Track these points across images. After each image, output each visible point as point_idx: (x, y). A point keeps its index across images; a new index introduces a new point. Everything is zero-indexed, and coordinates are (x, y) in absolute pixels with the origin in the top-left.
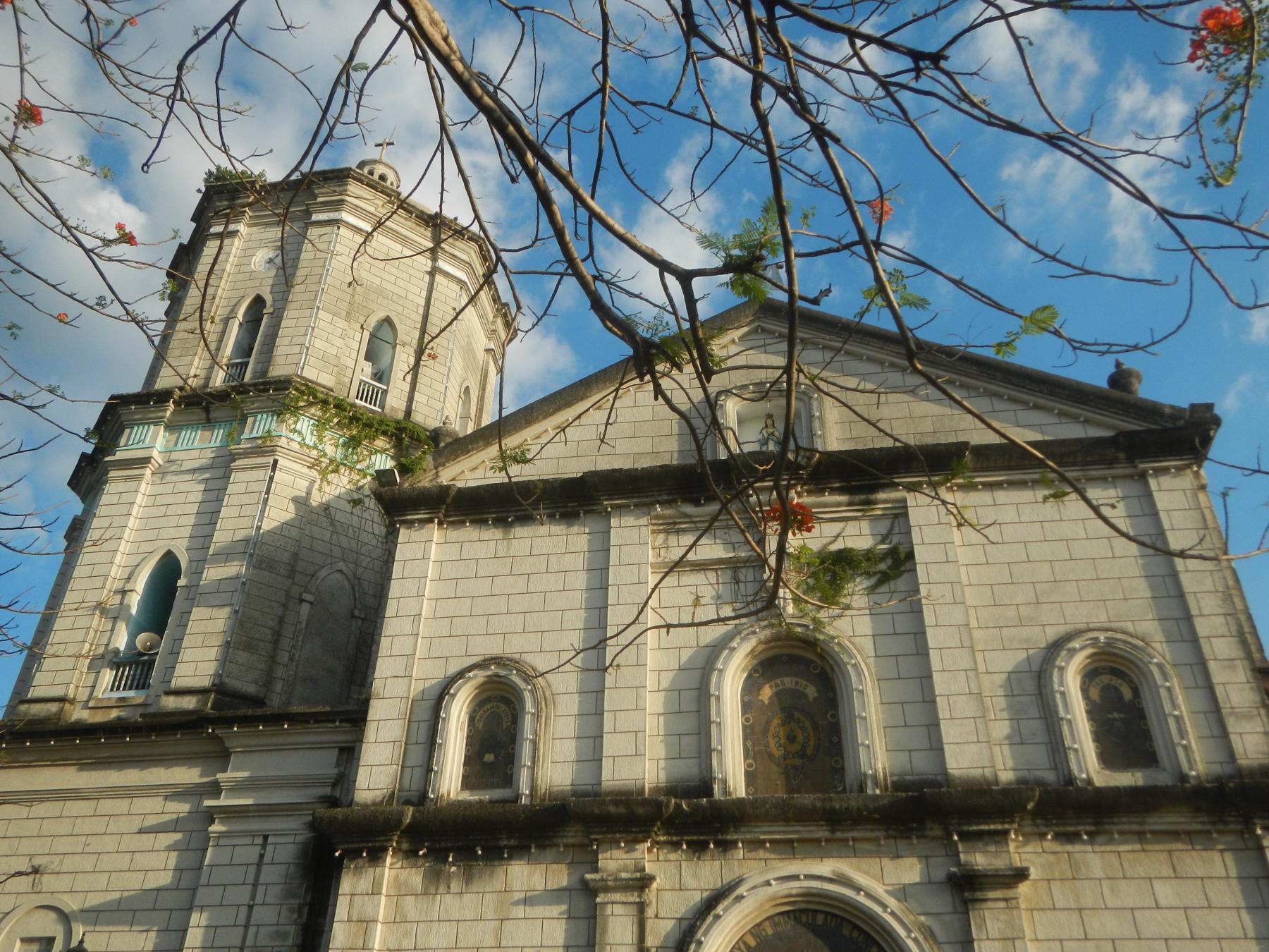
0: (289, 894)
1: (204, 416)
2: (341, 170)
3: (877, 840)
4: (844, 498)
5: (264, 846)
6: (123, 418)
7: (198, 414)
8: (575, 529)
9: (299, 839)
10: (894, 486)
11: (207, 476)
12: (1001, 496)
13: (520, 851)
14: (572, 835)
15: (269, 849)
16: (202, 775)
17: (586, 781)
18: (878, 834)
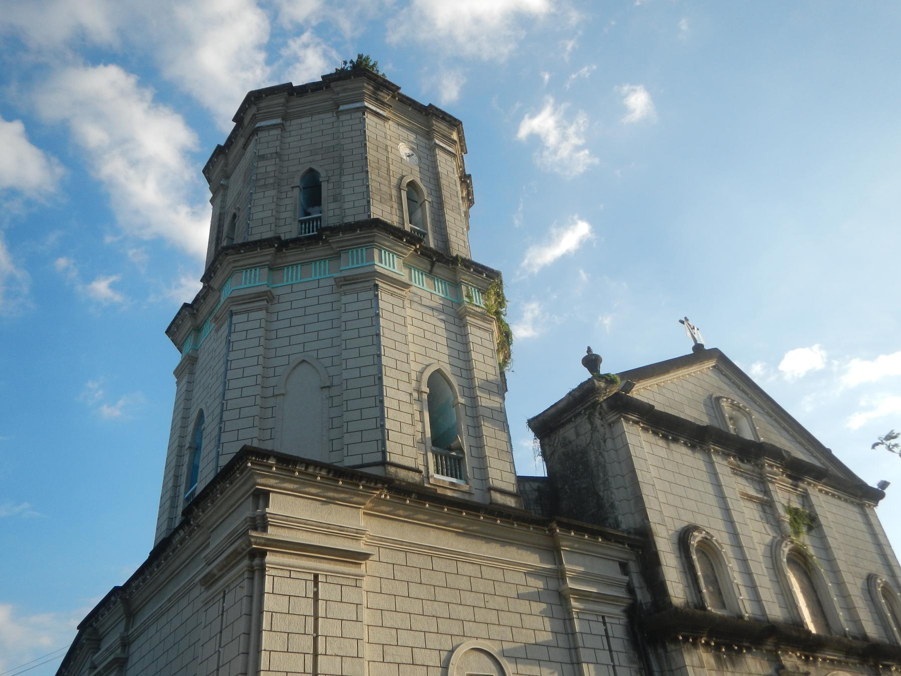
0: (631, 661)
1: (429, 267)
2: (456, 120)
3: (854, 664)
4: (790, 481)
5: (604, 623)
6: (376, 239)
7: (425, 264)
8: (698, 455)
9: (622, 622)
10: (803, 481)
11: (442, 317)
12: (829, 498)
13: (749, 650)
14: (769, 644)
15: (608, 626)
16: (542, 561)
17: (758, 612)
18: (857, 661)
